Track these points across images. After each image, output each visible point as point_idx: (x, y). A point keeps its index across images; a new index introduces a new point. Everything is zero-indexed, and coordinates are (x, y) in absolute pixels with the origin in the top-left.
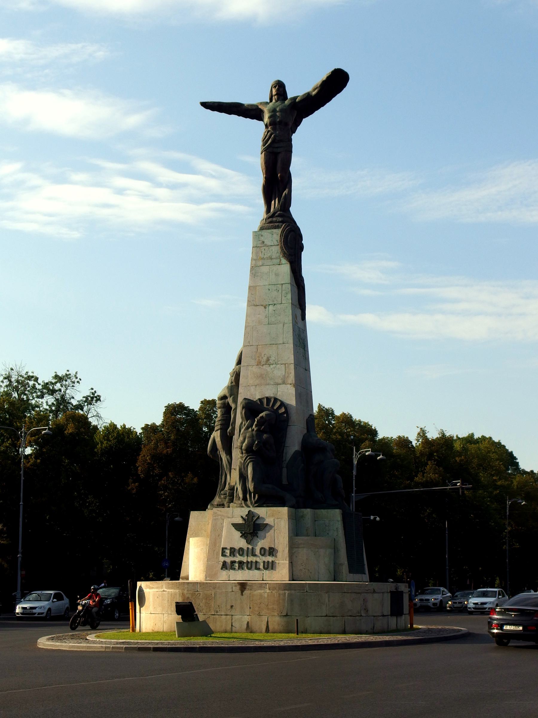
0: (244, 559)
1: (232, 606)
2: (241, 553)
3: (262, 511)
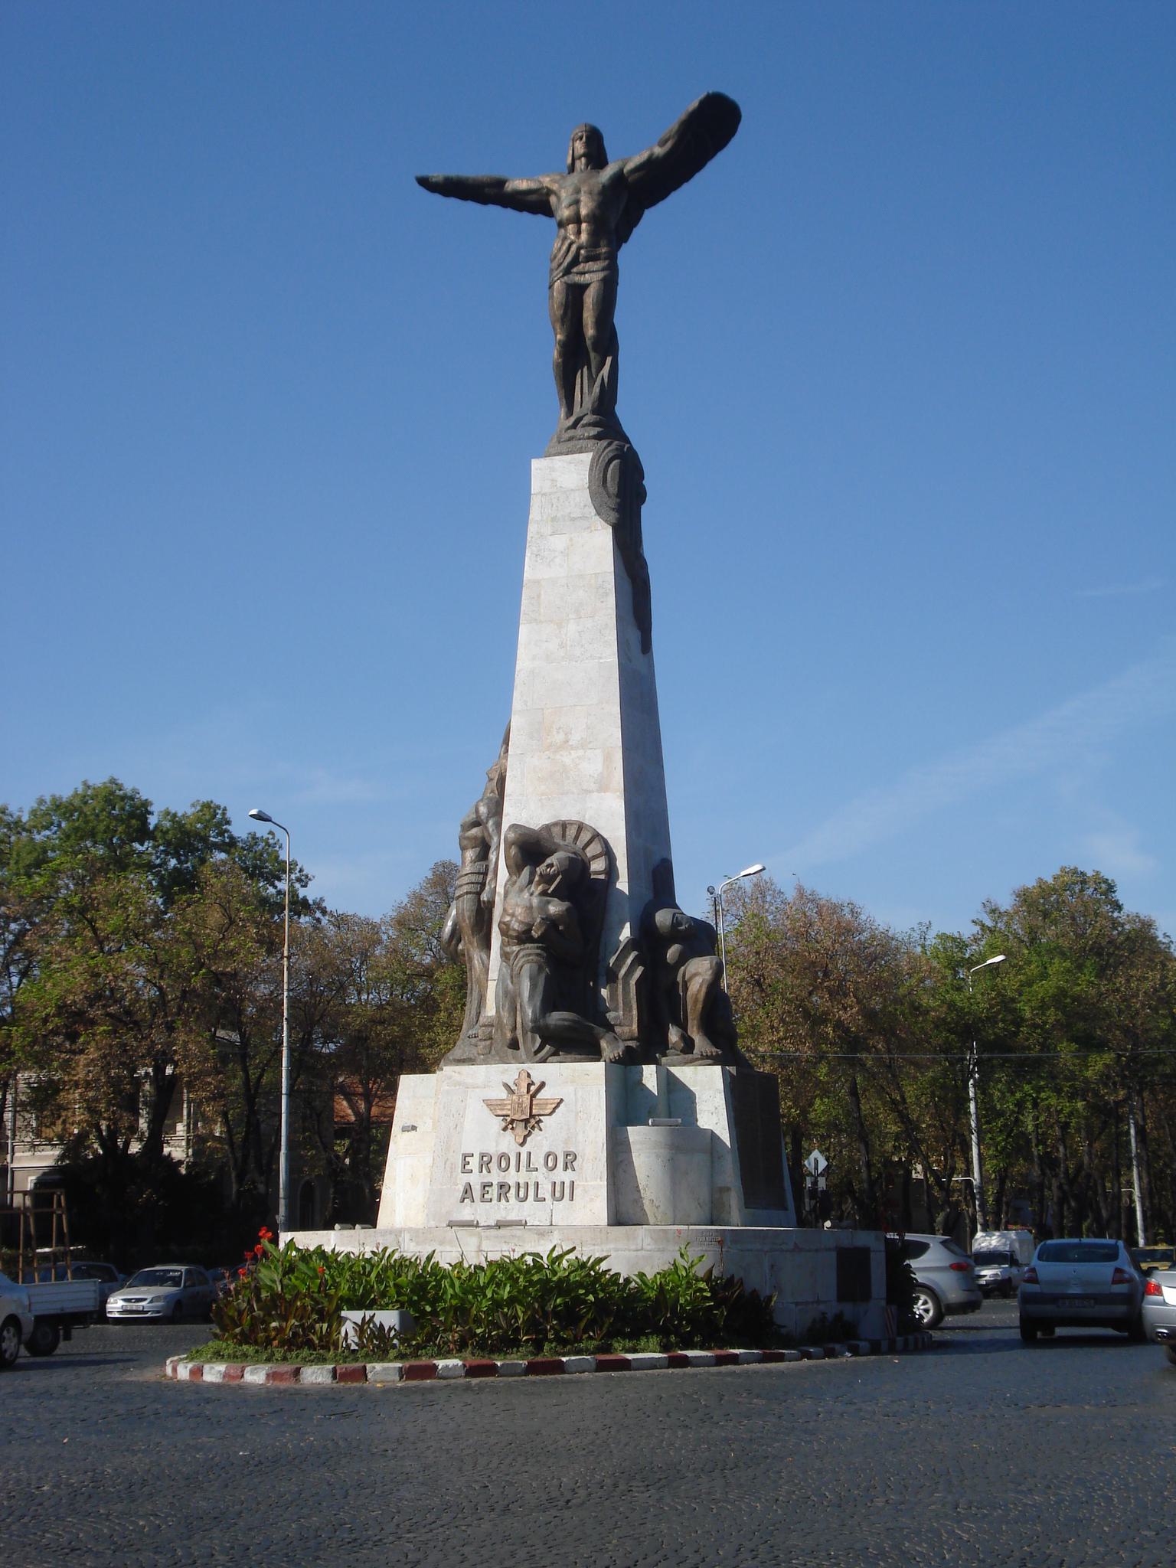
0: (512, 1177)
2: (503, 1164)
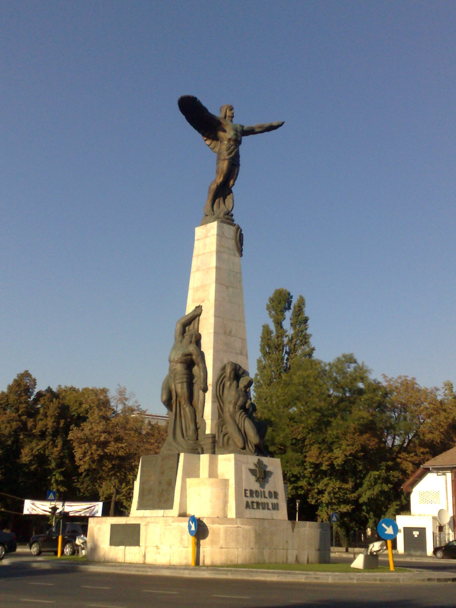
0: (260, 500)
1: (287, 541)
3: (266, 460)
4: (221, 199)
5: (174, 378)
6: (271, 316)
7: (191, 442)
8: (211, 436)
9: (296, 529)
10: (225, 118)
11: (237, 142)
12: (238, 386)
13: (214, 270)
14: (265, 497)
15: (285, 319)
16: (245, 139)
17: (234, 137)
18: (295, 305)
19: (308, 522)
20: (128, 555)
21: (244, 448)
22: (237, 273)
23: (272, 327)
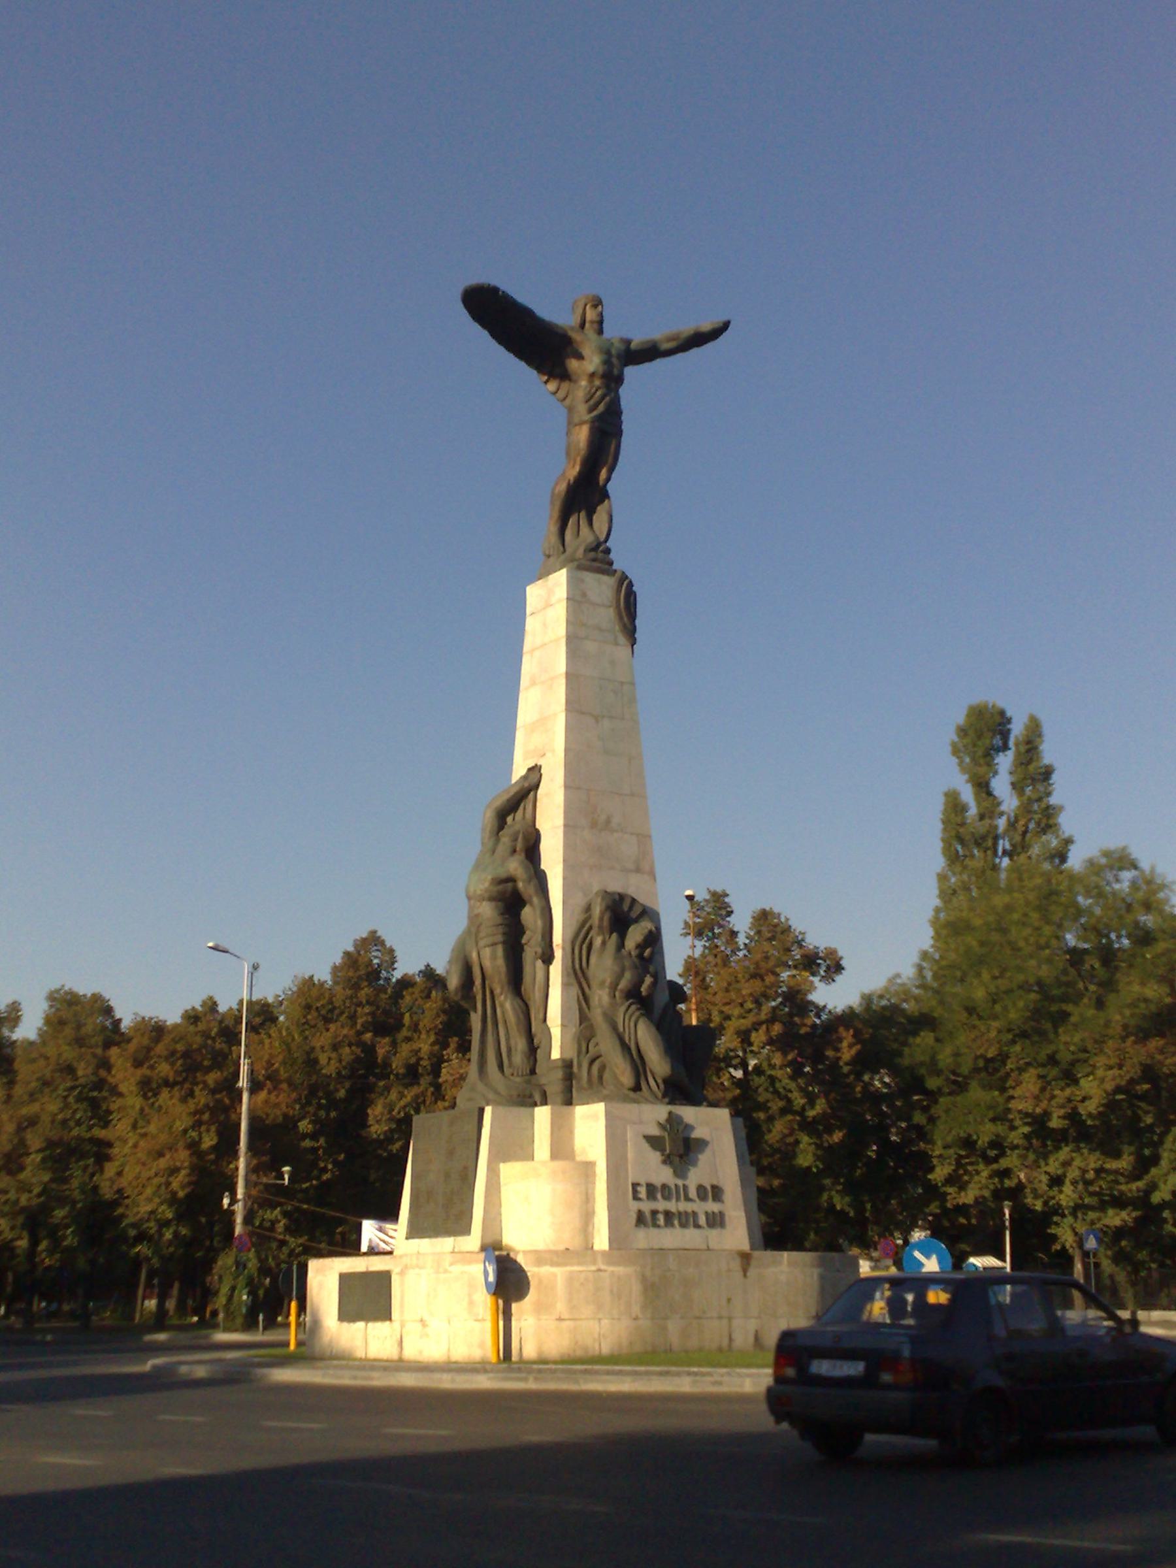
0: (672, 1206)
1: (729, 1300)
3: (688, 1113)
4: (583, 514)
5: (476, 937)
6: (963, 768)
7: (518, 1080)
8: (560, 1064)
9: (752, 1272)
10: (582, 325)
11: (612, 379)
12: (621, 945)
13: (563, 681)
14: (687, 1199)
15: (996, 773)
16: (630, 372)
17: (601, 370)
18: (1016, 737)
19: (785, 1254)
20: (370, 1340)
21: (637, 1088)
22: (622, 683)
23: (967, 794)
